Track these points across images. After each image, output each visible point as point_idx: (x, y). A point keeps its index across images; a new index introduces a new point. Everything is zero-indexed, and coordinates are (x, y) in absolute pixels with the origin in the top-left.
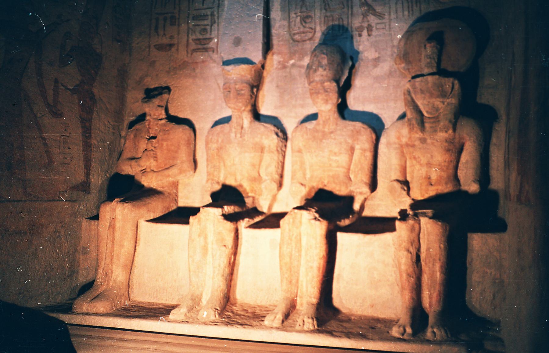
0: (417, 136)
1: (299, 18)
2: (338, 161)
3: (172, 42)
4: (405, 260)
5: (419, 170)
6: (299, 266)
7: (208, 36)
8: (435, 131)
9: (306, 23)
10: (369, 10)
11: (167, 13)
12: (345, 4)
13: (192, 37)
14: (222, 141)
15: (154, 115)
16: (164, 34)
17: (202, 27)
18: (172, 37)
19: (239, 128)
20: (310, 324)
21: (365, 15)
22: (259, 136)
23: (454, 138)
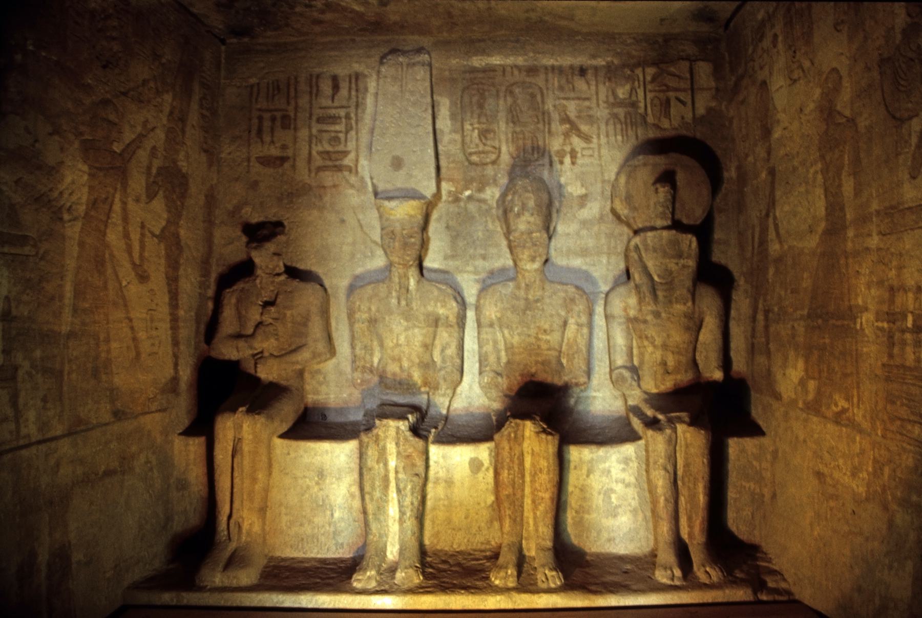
0: (650, 308)
1: (476, 131)
2: (549, 342)
3: (285, 154)
4: (661, 481)
5: (652, 353)
6: (523, 497)
7: (341, 148)
8: (670, 302)
9: (486, 138)
10: (571, 129)
11: (276, 110)
12: (540, 118)
13: (316, 149)
14: (378, 311)
15: (267, 267)
16: (273, 142)
17: (333, 134)
18: (284, 147)
19: (403, 291)
20: (555, 579)
21: (567, 135)
22: (432, 303)
23: (693, 313)
